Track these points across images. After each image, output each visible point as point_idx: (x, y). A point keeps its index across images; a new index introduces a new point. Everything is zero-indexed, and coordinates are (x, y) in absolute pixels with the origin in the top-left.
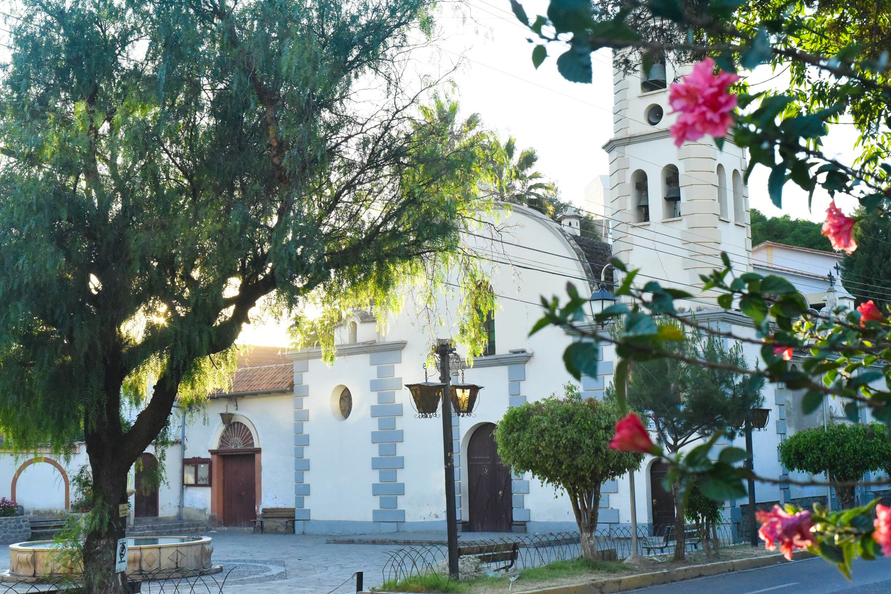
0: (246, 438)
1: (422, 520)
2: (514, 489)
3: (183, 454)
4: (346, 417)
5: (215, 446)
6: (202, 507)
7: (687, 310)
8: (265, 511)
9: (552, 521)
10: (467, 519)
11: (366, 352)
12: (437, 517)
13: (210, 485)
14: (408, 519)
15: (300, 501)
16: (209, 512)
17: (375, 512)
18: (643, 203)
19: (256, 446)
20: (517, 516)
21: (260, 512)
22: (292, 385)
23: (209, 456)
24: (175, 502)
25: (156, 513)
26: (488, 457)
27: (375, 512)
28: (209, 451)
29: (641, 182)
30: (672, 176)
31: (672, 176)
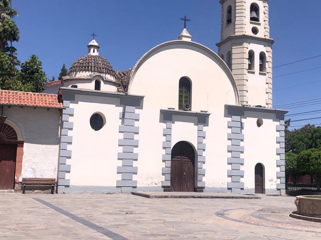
0: (8, 135)
1: (147, 186)
2: (199, 173)
7: (266, 107)
8: (24, 180)
9: (215, 187)
12: (156, 184)
14: (138, 185)
17: (118, 181)
18: (250, 63)
19: (19, 140)
21: (20, 180)
27: (118, 181)
29: (251, 55)
30: (262, 56)
31: (262, 56)
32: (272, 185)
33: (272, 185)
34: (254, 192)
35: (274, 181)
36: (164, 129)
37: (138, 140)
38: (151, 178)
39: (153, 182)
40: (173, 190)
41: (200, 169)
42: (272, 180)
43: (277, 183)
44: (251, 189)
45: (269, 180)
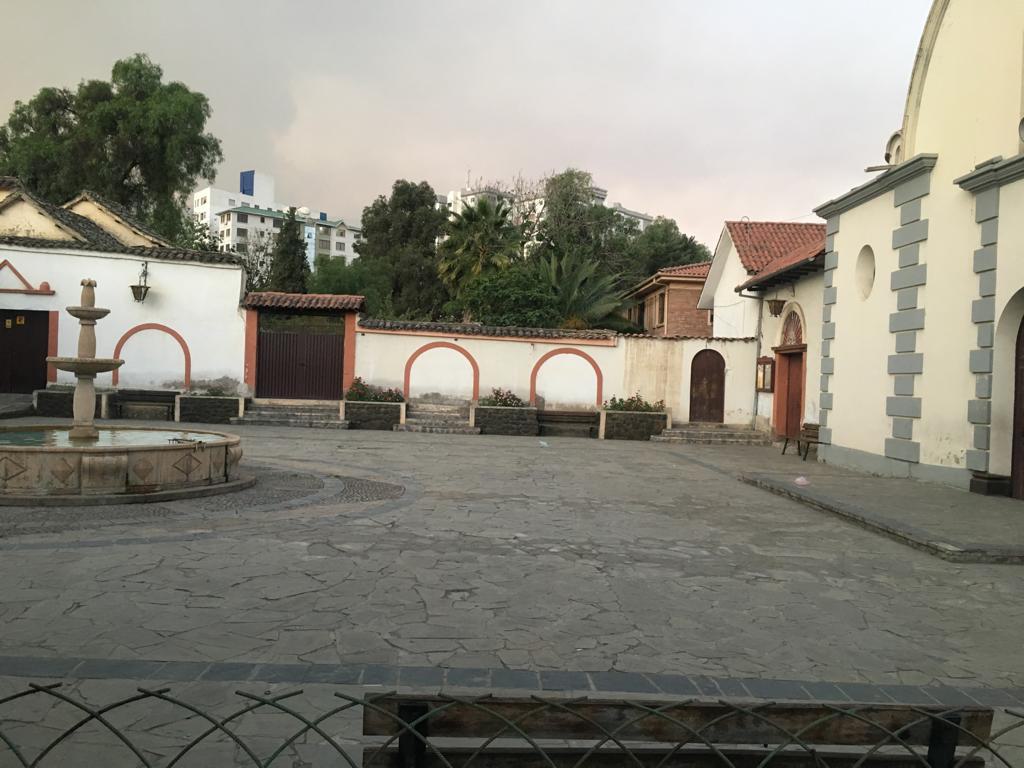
1: (938, 464)
3: (759, 353)
4: (867, 297)
5: (777, 343)
6: (767, 416)
8: (806, 425)
10: (1007, 472)
11: (889, 188)
13: (772, 390)
14: (923, 460)
15: (823, 416)
16: (771, 423)
17: (888, 441)
22: (822, 254)
23: (772, 355)
24: (748, 407)
25: (722, 421)
28: (773, 348)
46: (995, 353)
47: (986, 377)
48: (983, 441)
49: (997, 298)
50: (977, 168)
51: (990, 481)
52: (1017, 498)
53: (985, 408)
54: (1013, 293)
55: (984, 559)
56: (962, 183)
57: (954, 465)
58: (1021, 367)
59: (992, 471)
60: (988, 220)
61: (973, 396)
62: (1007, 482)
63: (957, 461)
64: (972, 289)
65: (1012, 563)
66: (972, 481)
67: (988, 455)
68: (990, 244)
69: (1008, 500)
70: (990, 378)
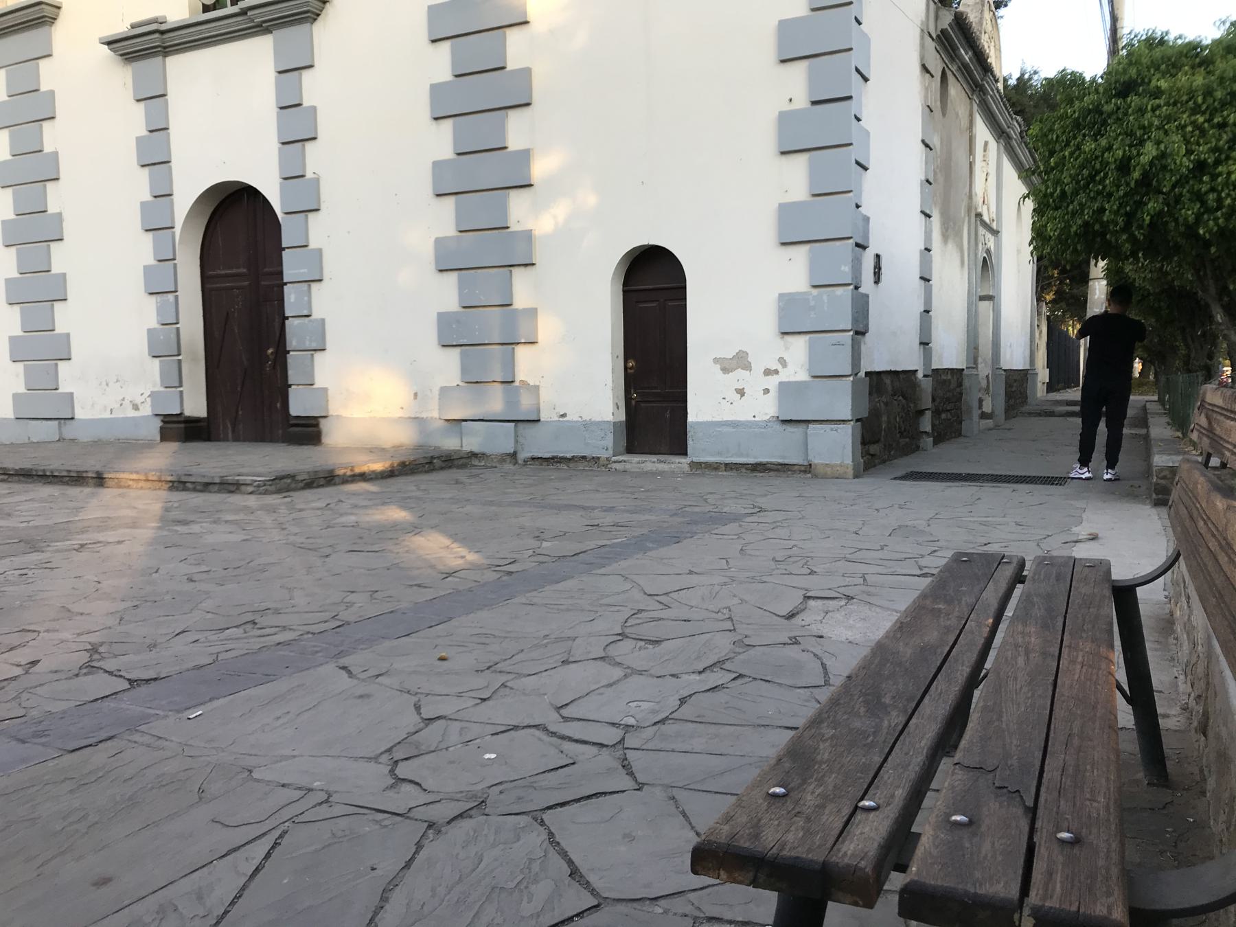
1: (107, 415)
2: (292, 341)
12: (136, 407)
14: (80, 414)
17: (16, 396)
20: (298, 406)
26: (245, 270)
32: (741, 392)
33: (741, 392)
34: (609, 441)
35: (758, 367)
36: (139, 139)
37: (60, 214)
38: (117, 381)
39: (123, 399)
40: (230, 435)
41: (297, 321)
42: (741, 361)
43: (786, 375)
44: (587, 425)
45: (716, 360)
46: (178, 266)
47: (171, 297)
48: (174, 379)
49: (176, 198)
50: (133, 26)
51: (188, 425)
52: (218, 440)
53: (173, 336)
54: (201, 192)
55: (293, 485)
56: (109, 43)
57: (132, 413)
58: (208, 286)
59: (187, 413)
60: (153, 97)
61: (153, 323)
62: (202, 424)
63: (136, 407)
64: (140, 185)
65: (319, 486)
66: (161, 428)
67: (181, 392)
68: (159, 130)
69: (209, 443)
70: (177, 297)
